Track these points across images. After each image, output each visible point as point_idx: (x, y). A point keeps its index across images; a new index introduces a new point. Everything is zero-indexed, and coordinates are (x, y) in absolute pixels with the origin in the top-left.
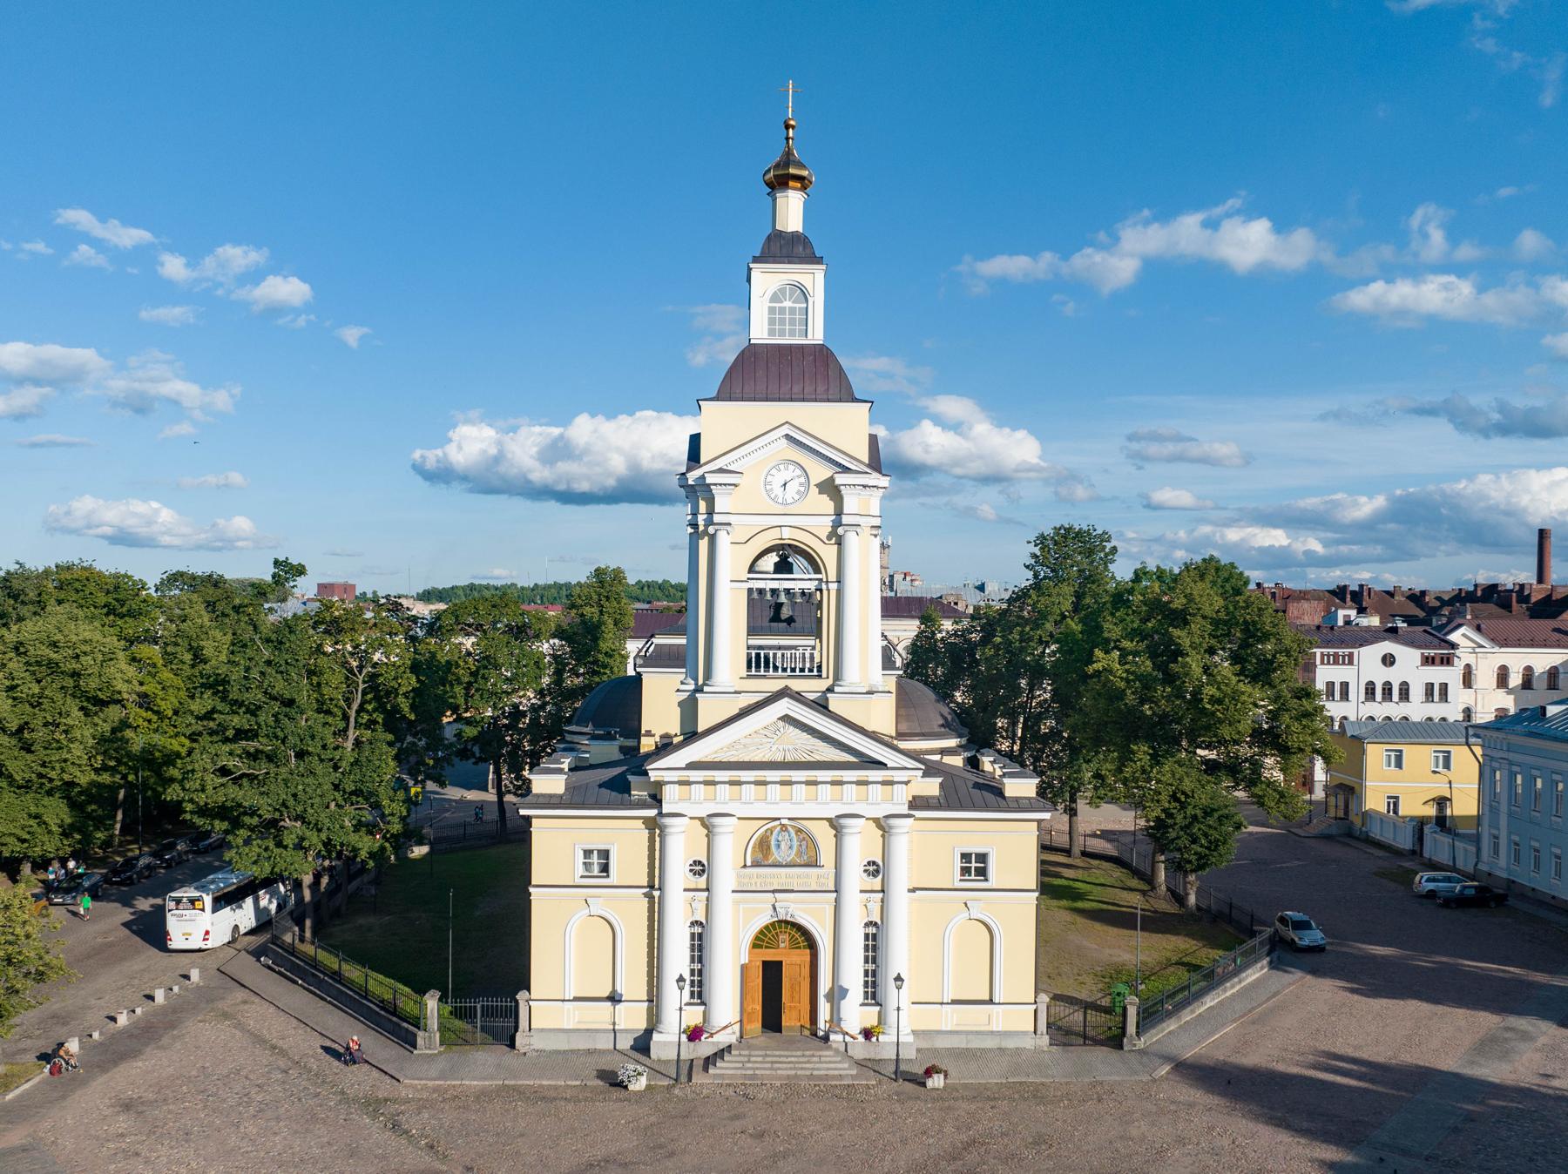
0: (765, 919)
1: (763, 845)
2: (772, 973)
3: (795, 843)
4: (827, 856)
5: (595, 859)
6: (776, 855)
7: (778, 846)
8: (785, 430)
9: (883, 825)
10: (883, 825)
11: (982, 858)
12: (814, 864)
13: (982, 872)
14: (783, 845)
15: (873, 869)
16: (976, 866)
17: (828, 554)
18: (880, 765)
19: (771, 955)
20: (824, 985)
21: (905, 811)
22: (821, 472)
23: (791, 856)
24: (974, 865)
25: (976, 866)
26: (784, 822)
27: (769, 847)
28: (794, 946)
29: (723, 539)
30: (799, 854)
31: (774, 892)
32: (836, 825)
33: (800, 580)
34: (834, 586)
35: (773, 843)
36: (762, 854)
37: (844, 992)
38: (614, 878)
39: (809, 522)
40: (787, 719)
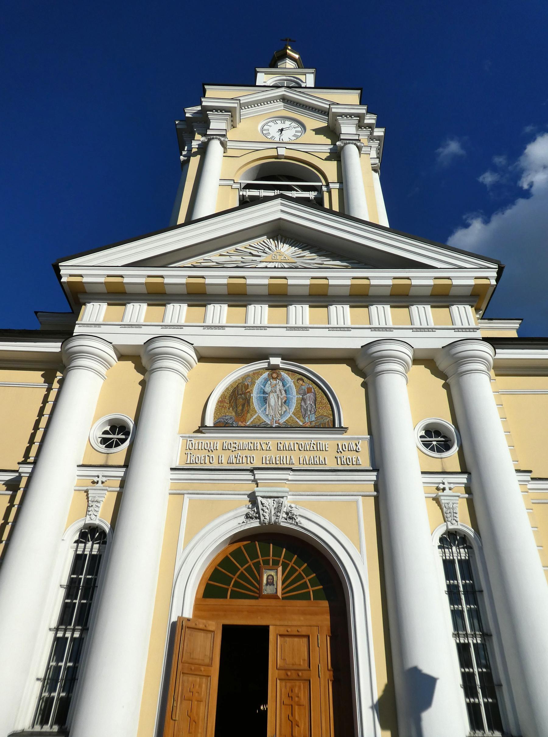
0: (232, 521)
1: (237, 400)
2: (244, 656)
3: (295, 397)
6: (259, 413)
7: (265, 400)
9: (444, 365)
12: (331, 425)
14: (272, 399)
19: (243, 613)
20: (370, 680)
26: (275, 361)
27: (247, 401)
28: (294, 592)
30: (301, 411)
31: (252, 471)
32: (364, 363)
34: (335, 187)
35: (255, 395)
37: (422, 688)
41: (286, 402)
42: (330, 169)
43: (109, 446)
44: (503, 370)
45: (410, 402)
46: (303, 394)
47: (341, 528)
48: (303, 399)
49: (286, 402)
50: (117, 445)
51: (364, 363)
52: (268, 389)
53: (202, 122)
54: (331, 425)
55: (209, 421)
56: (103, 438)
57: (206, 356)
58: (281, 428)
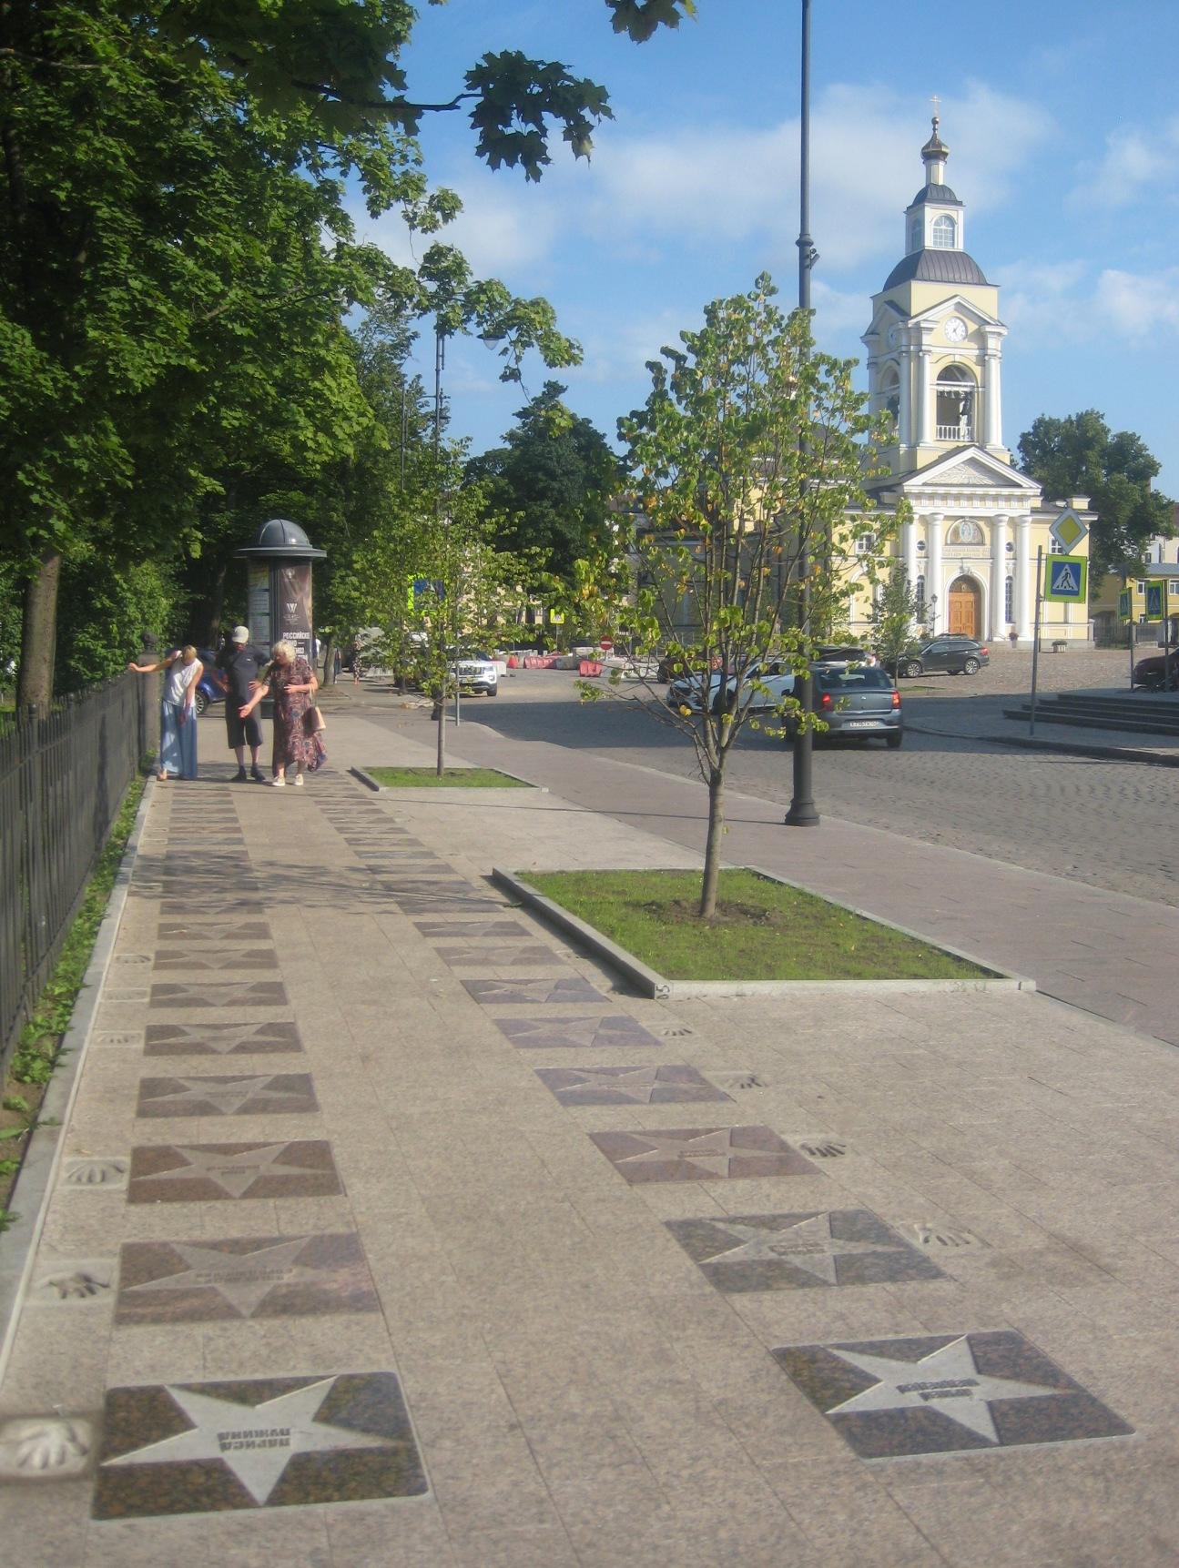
0: (957, 574)
4: (987, 540)
6: (963, 538)
8: (956, 300)
9: (1015, 524)
10: (1015, 524)
12: (982, 544)
15: (1010, 547)
17: (977, 370)
22: (973, 327)
23: (970, 539)
29: (927, 359)
33: (962, 387)
36: (955, 539)
39: (967, 355)
40: (973, 462)
42: (977, 370)
44: (1034, 522)
45: (1005, 534)
47: (982, 575)
51: (993, 522)
53: (919, 329)
54: (982, 544)
57: (947, 518)
58: (970, 544)
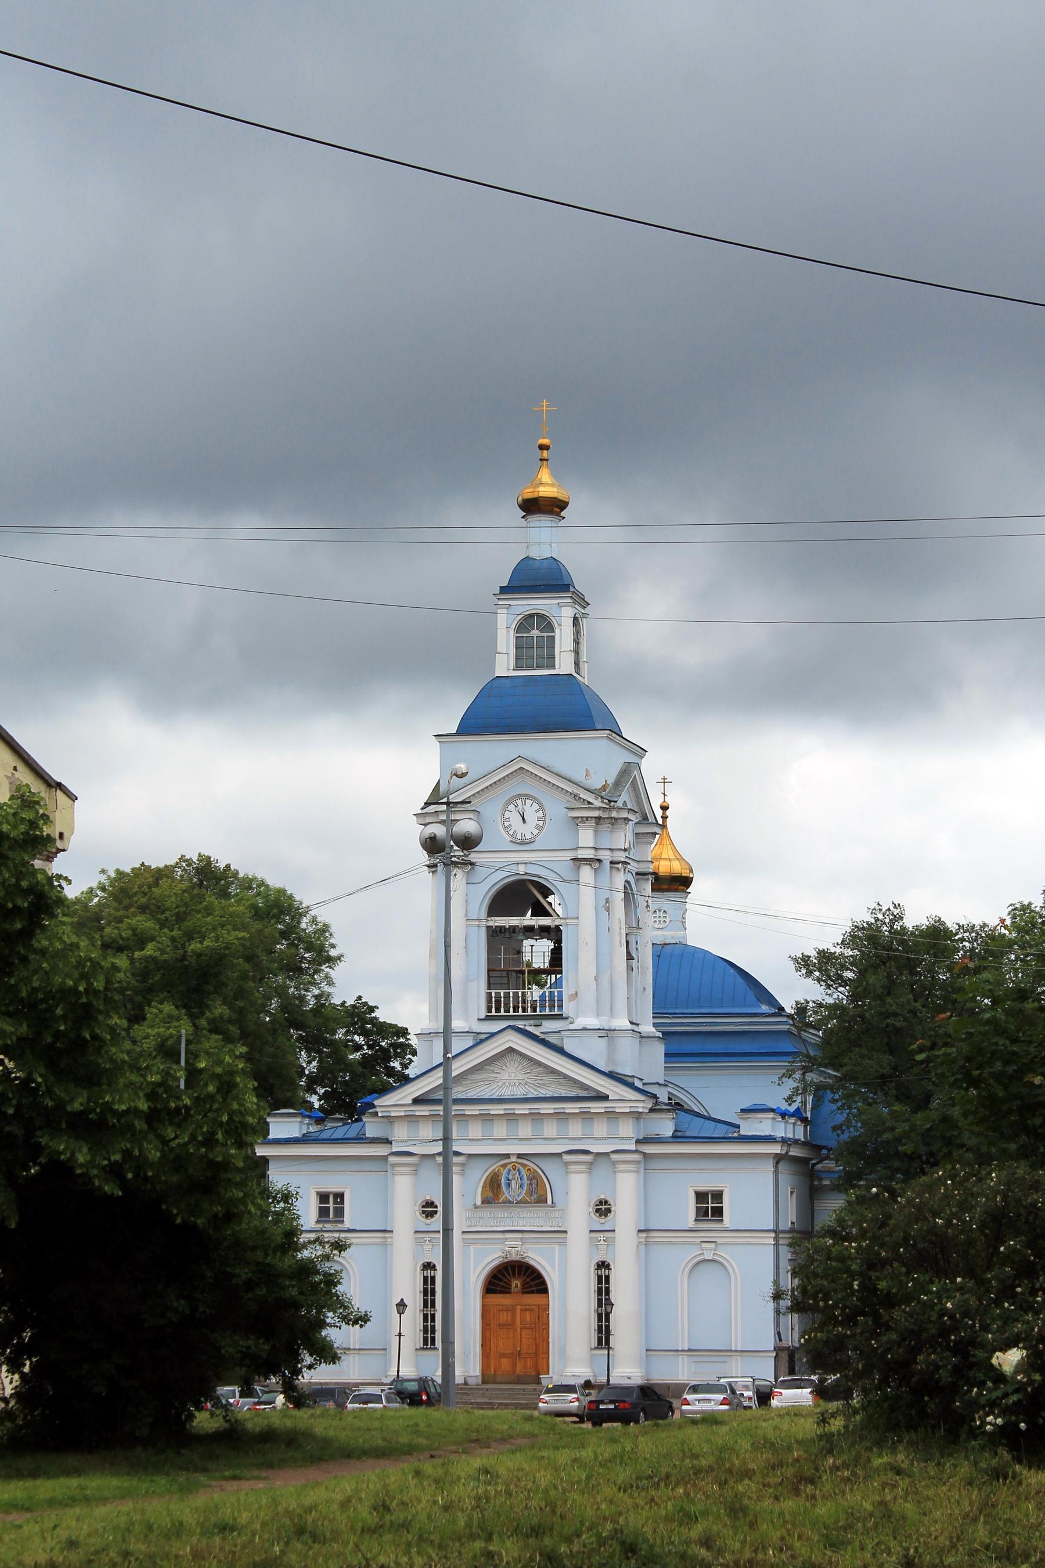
3: (526, 1182)
5: (331, 1205)
6: (505, 1194)
7: (509, 1185)
11: (718, 1196)
13: (718, 1212)
14: (513, 1184)
16: (709, 1206)
18: (605, 1098)
21: (633, 1147)
24: (710, 1205)
25: (709, 1206)
27: (499, 1185)
30: (530, 1193)
35: (503, 1181)
38: (348, 1223)
41: (521, 1186)
43: (427, 1217)
46: (530, 1179)
48: (531, 1184)
49: (521, 1186)
50: (432, 1216)
52: (510, 1177)
55: (479, 1202)
56: (424, 1212)
